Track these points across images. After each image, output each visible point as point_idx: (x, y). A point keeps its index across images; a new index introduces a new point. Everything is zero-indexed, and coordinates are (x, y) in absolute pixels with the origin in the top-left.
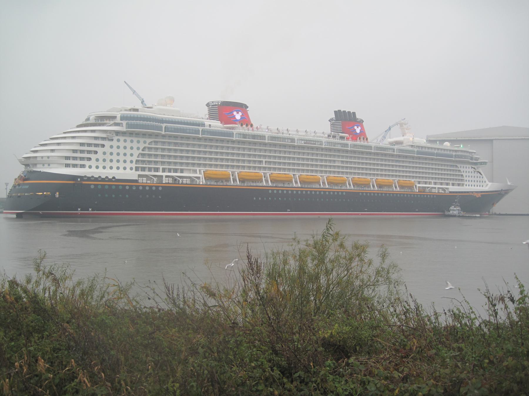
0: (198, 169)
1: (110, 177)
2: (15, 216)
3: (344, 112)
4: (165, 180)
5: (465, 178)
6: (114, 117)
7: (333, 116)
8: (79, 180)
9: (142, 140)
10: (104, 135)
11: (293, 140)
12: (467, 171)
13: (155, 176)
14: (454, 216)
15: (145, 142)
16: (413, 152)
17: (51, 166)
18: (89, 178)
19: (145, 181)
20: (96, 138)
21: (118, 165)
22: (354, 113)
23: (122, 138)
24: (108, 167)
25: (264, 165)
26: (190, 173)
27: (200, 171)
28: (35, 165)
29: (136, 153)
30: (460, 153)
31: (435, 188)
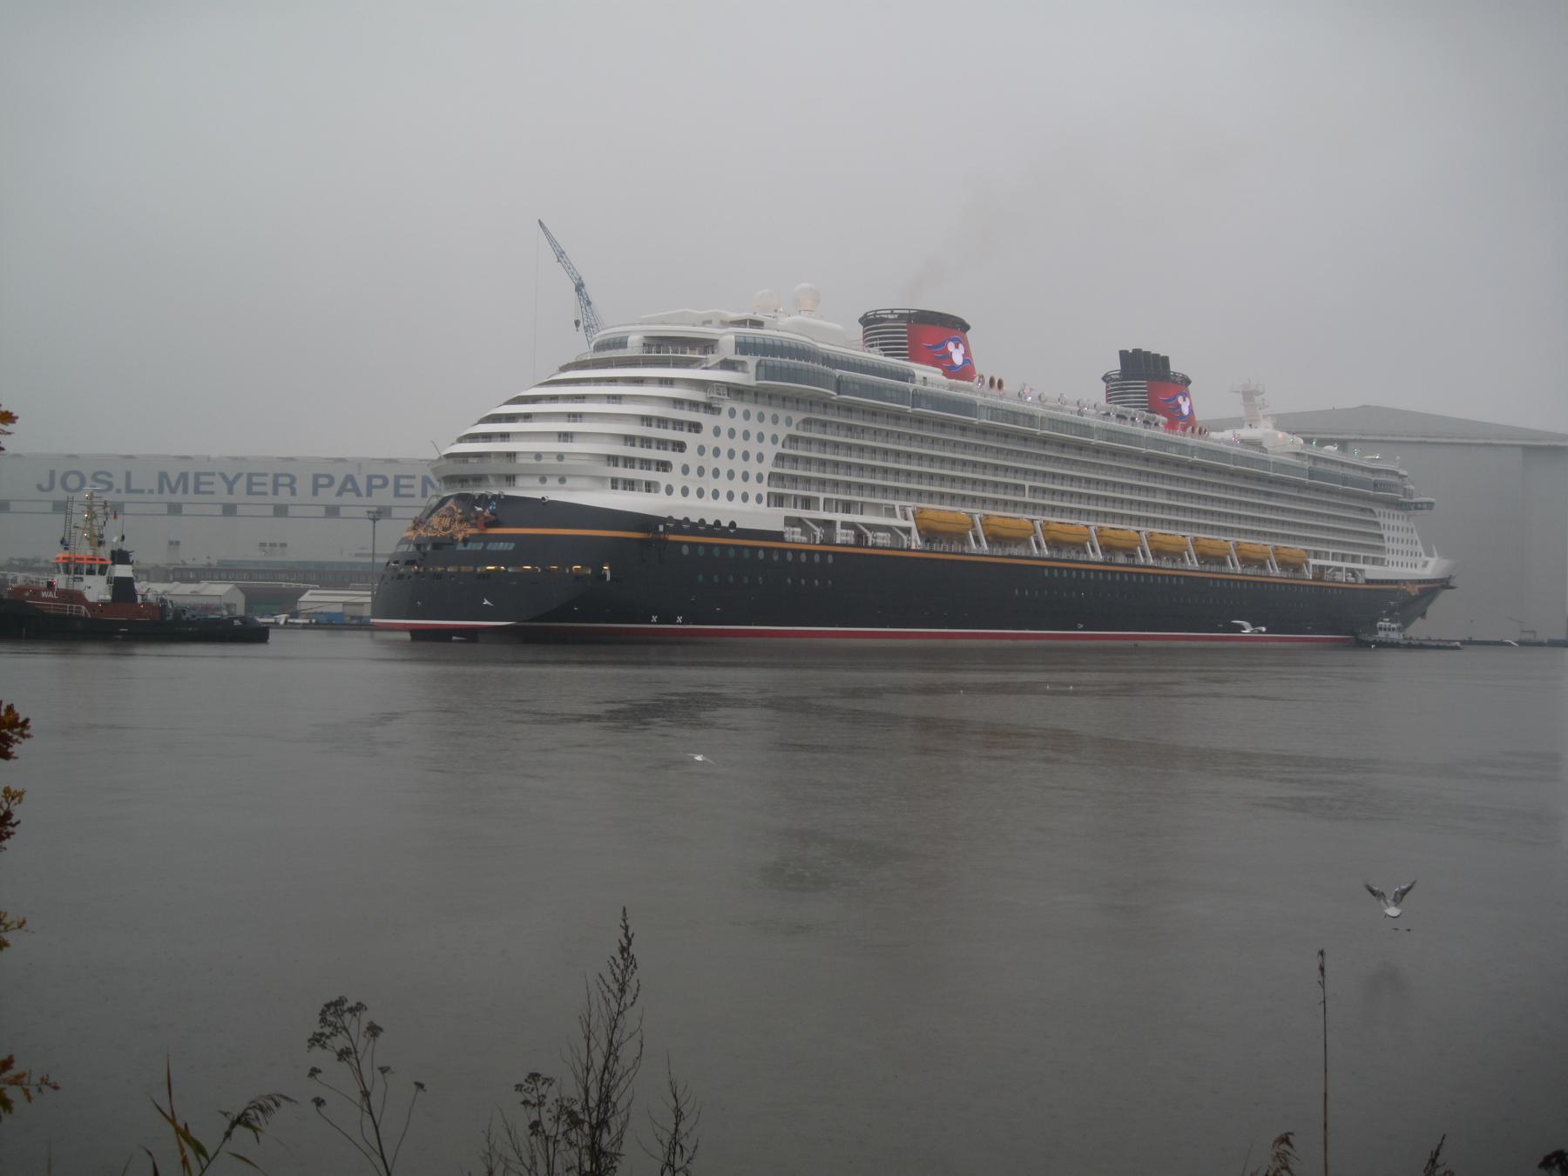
0: (897, 504)
1: (695, 519)
2: (407, 636)
3: (1148, 353)
4: (842, 536)
5: (1387, 545)
6: (708, 345)
7: (1115, 365)
8: (661, 528)
9: (783, 414)
10: (699, 396)
11: (1086, 429)
12: (1392, 524)
13: (818, 522)
14: (1394, 645)
15: (789, 422)
16: (1299, 469)
17: (569, 482)
18: (678, 523)
19: (797, 537)
20: (677, 402)
21: (725, 488)
22: (1165, 360)
23: (740, 408)
24: (708, 493)
25: (1027, 499)
26: (878, 514)
27: (903, 509)
28: (510, 479)
29: (770, 451)
30: (1383, 478)
31: (1340, 569)
